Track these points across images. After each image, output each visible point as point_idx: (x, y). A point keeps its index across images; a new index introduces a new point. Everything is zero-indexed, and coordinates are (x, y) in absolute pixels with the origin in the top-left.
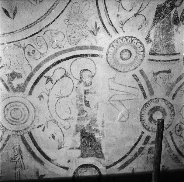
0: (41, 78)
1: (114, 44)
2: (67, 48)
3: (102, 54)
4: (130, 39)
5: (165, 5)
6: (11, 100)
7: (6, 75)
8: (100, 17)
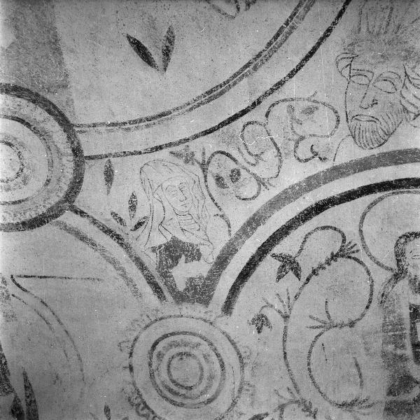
0: (260, 260)
2: (347, 160)
6: (171, 326)
7: (154, 250)
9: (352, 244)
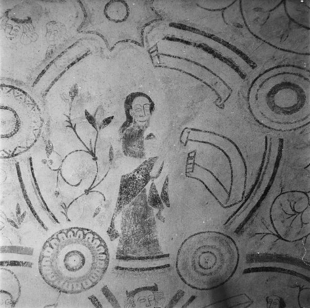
1: (53, 242)
3: (31, 261)
4: (80, 233)
5: (134, 175)
8: (25, 196)
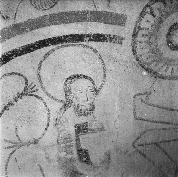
3: (122, 35)
9: (33, 85)
